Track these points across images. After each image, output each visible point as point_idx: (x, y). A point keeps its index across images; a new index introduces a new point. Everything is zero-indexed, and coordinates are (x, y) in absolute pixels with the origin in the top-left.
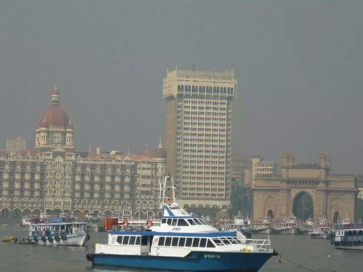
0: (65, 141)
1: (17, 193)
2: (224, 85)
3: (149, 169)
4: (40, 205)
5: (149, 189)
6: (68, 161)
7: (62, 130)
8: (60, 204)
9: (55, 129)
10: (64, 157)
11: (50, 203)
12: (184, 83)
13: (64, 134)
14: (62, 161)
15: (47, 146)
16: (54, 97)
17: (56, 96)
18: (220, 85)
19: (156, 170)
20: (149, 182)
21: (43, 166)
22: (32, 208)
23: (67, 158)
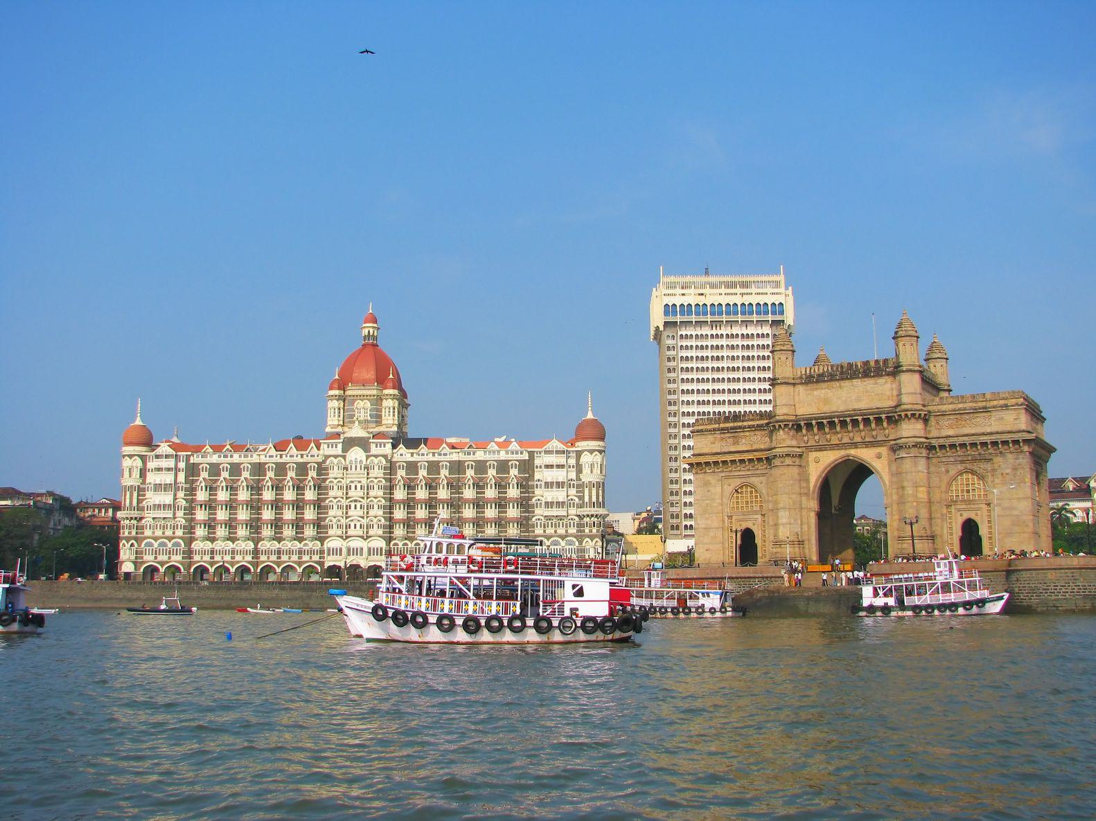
0: (380, 417)
1: (267, 532)
2: (762, 300)
3: (560, 466)
4: (316, 558)
5: (562, 512)
6: (376, 456)
7: (375, 392)
8: (361, 555)
9: (360, 392)
10: (366, 448)
11: (338, 551)
12: (678, 301)
13: (379, 399)
14: (364, 459)
15: (340, 429)
16: (368, 329)
17: (371, 325)
18: (754, 300)
19: (579, 469)
20: (559, 495)
21: (322, 469)
22: (300, 564)
23: (374, 450)
